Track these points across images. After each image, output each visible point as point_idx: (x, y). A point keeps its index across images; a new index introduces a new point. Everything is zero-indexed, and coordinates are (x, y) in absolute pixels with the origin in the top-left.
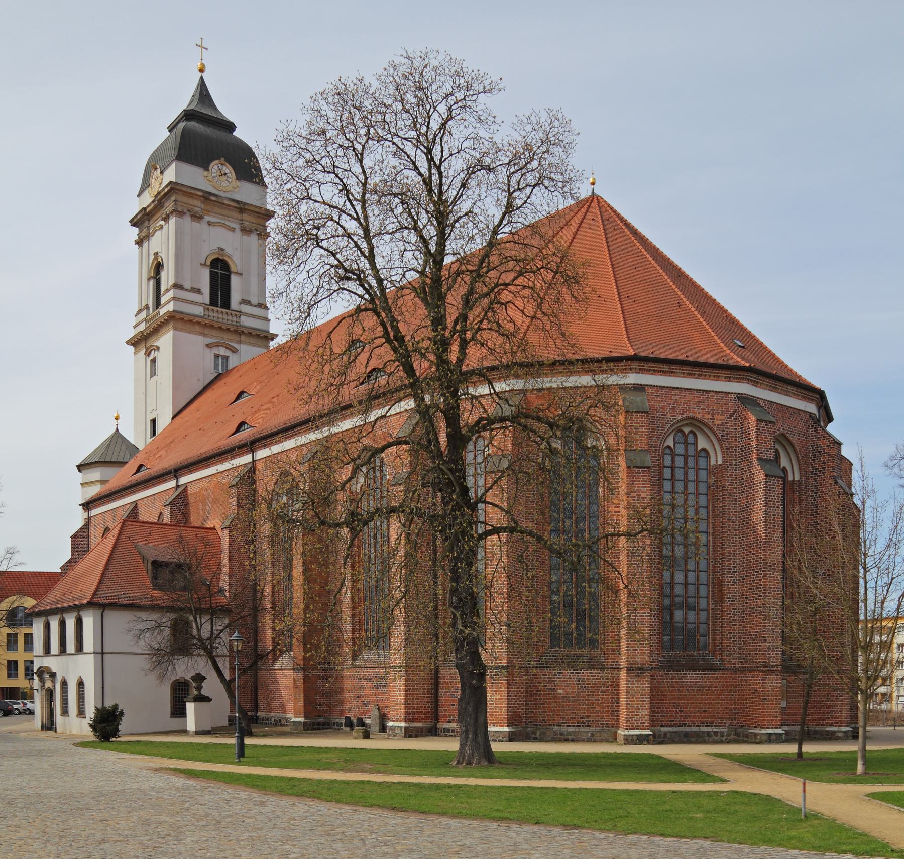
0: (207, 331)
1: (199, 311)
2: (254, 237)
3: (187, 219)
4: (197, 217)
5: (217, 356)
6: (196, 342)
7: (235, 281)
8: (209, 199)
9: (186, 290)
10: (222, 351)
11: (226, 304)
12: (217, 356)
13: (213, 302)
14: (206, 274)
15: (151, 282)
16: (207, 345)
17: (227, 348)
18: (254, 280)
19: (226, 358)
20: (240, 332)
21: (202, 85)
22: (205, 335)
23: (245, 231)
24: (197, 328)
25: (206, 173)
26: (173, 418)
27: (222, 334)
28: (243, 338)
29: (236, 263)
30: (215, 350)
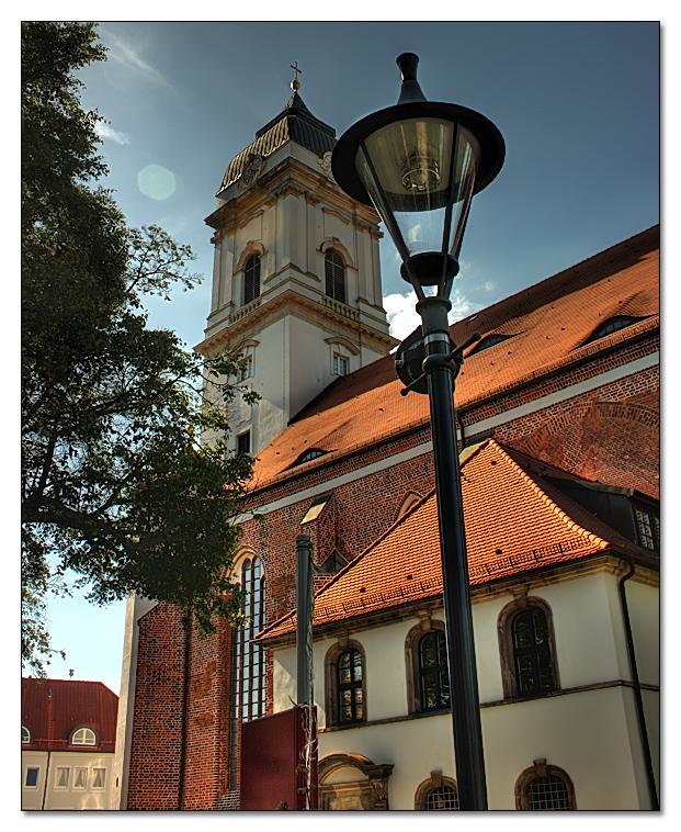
0: (325, 324)
1: (318, 298)
2: (366, 235)
3: (302, 198)
4: (312, 200)
5: (336, 356)
6: (312, 335)
7: (350, 276)
8: (325, 186)
9: (302, 272)
10: (343, 351)
11: (342, 296)
12: (336, 356)
13: (329, 293)
14: (321, 261)
15: (240, 277)
16: (327, 340)
17: (347, 347)
18: (369, 279)
19: (345, 361)
20: (360, 331)
21: (297, 97)
22: (324, 329)
23: (357, 224)
24: (315, 317)
25: (320, 161)
26: (292, 422)
27: (346, 333)
28: (363, 339)
29: (350, 254)
30: (334, 348)
